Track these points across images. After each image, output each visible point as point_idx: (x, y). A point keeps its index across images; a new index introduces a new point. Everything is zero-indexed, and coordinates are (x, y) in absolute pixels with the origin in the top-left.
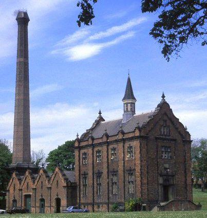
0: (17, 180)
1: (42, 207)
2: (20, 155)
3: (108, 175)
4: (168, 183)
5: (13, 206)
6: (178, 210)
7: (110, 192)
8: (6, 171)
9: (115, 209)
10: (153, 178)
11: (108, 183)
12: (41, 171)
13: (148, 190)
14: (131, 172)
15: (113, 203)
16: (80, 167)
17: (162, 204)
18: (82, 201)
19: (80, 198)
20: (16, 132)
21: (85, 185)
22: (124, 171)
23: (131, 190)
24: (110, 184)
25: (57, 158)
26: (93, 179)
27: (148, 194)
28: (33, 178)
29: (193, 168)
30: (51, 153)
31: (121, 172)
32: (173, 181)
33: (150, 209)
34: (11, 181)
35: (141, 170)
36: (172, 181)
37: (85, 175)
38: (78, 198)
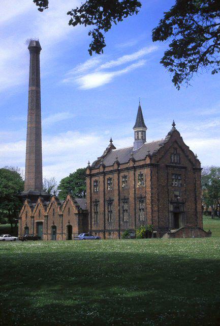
0: (29, 207)
1: (54, 234)
2: (32, 182)
3: (119, 203)
4: (178, 210)
5: (25, 233)
6: (188, 237)
7: (121, 219)
8: (18, 199)
9: (126, 236)
10: (164, 205)
11: (119, 211)
12: (53, 199)
13: (159, 218)
14: (142, 199)
15: (124, 230)
16: (91, 195)
17: (173, 231)
18: (93, 228)
19: (91, 225)
20: (28, 160)
21: (96, 213)
22: (135, 199)
23: (142, 218)
24: (121, 212)
25: (68, 185)
26: (105, 206)
27: (159, 222)
28: (45, 206)
29: (203, 196)
30: (63, 180)
31: (131, 200)
32: (184, 208)
33: (161, 236)
34: (23, 208)
35: (151, 197)
36: (182, 208)
37: (96, 202)
38: (90, 226)
